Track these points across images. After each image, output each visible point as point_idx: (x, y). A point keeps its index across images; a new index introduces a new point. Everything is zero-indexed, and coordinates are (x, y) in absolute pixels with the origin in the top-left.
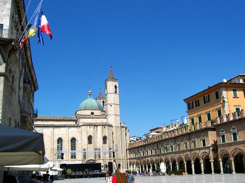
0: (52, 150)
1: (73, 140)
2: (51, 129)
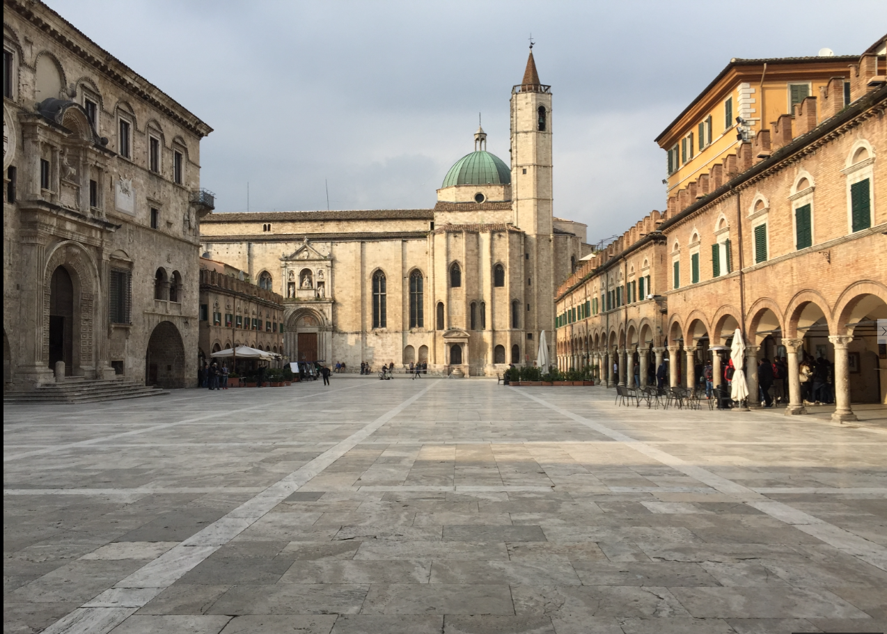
0: (356, 303)
1: (415, 279)
2: (354, 246)
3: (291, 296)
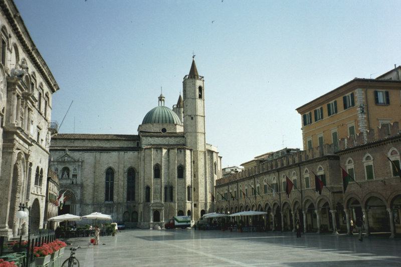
1: (132, 173)
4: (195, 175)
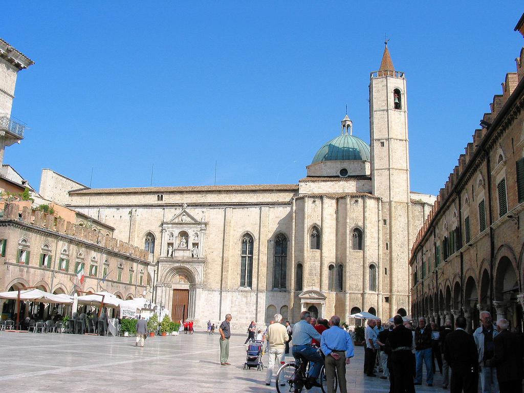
3: (169, 256)
4: (388, 246)
